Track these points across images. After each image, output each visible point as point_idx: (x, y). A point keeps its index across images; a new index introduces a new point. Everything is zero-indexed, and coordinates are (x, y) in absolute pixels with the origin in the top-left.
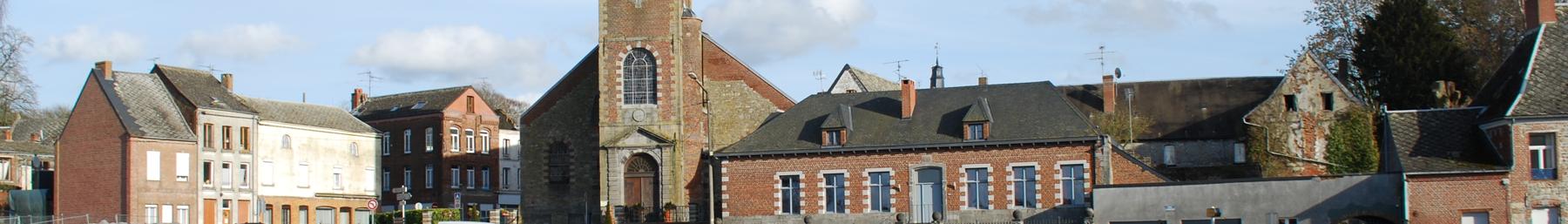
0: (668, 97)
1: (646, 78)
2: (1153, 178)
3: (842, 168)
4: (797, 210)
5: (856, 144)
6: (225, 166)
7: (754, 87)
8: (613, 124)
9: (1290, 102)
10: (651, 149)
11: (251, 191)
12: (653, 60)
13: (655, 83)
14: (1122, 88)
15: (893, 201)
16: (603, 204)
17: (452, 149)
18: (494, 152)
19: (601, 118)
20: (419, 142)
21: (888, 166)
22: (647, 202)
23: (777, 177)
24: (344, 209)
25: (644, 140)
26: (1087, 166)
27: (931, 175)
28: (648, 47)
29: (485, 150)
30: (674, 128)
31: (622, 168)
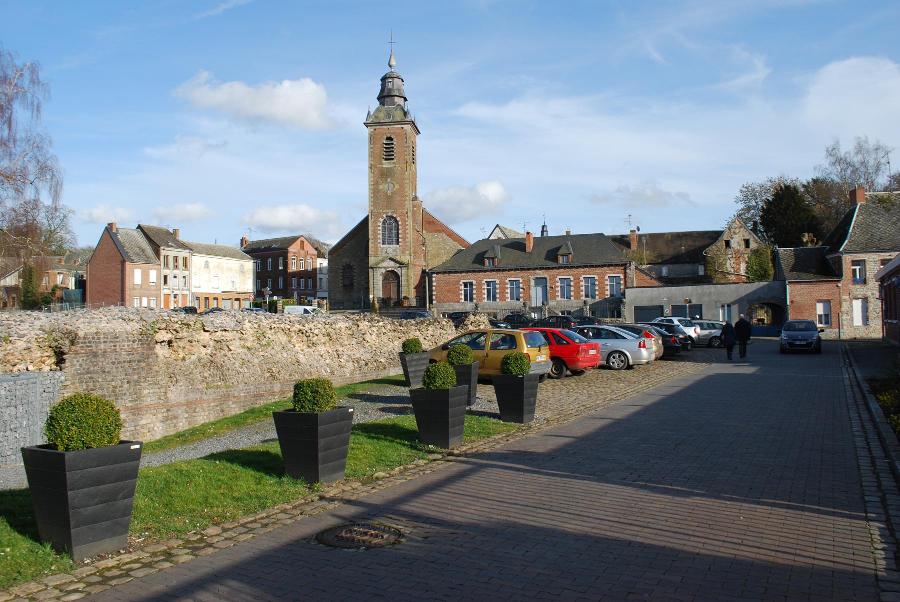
0: (405, 241)
1: (393, 232)
2: (657, 283)
3: (495, 278)
4: (472, 300)
5: (503, 265)
6: (175, 277)
7: (449, 236)
9: (728, 244)
11: (188, 290)
12: (397, 222)
13: (398, 234)
14: (640, 236)
15: (521, 295)
16: (371, 296)
17: (293, 268)
18: (315, 270)
19: (370, 252)
20: (275, 264)
21: (519, 277)
22: (394, 296)
23: (461, 283)
24: (237, 299)
25: (392, 264)
26: (622, 277)
27: (541, 281)
29: (310, 269)
30: (408, 257)
31: (381, 278)
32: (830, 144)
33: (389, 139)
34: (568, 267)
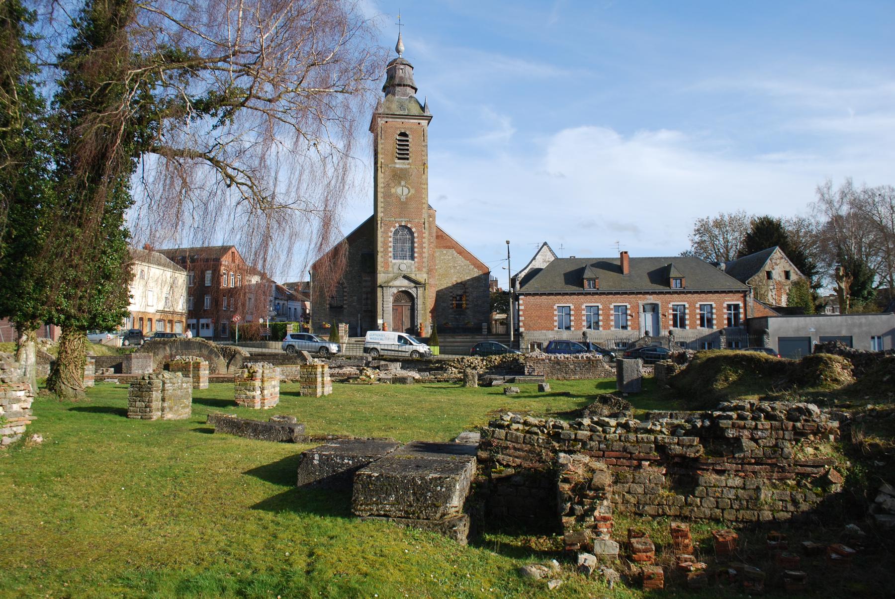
3: (598, 302)
7: (460, 253)
9: (769, 275)
10: (410, 288)
12: (412, 233)
15: (629, 323)
19: (379, 268)
21: (626, 302)
23: (555, 307)
25: (406, 283)
26: (741, 305)
27: (654, 308)
28: (409, 226)
30: (425, 276)
31: (391, 299)
32: (822, 184)
33: (403, 134)
34: (683, 293)
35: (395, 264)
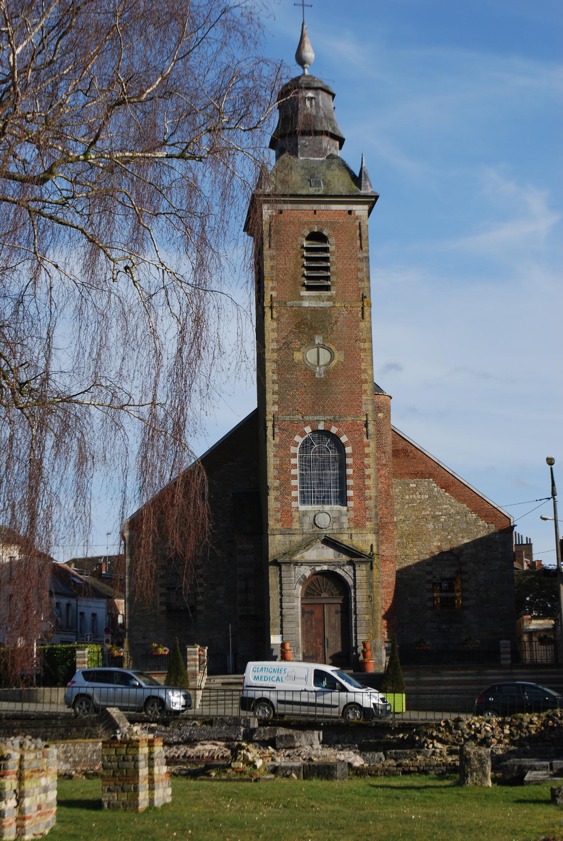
8: (287, 532)
10: (340, 565)
12: (340, 447)
19: (271, 522)
25: (329, 554)
28: (334, 430)
30: (371, 538)
31: (299, 590)
35: (305, 513)
